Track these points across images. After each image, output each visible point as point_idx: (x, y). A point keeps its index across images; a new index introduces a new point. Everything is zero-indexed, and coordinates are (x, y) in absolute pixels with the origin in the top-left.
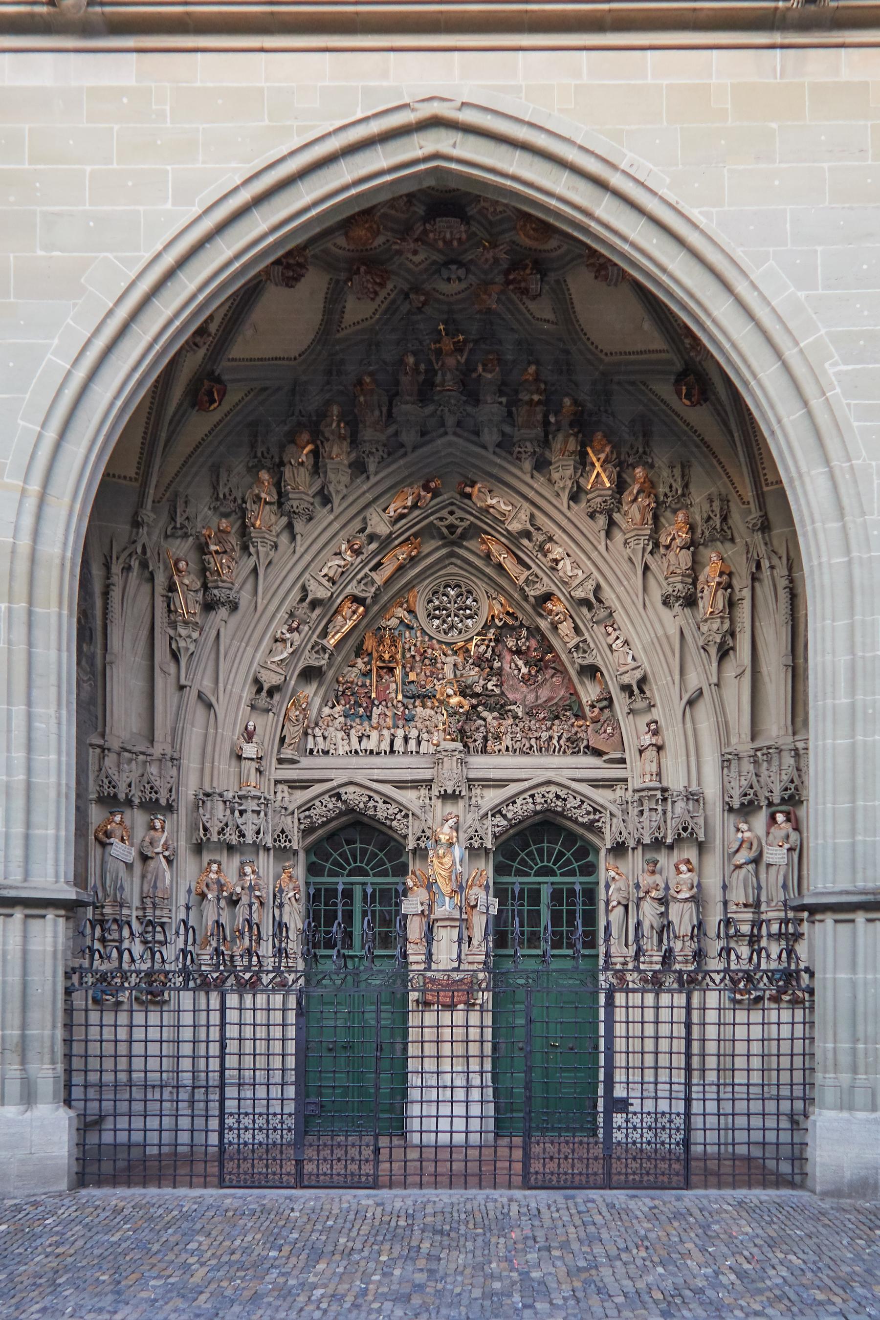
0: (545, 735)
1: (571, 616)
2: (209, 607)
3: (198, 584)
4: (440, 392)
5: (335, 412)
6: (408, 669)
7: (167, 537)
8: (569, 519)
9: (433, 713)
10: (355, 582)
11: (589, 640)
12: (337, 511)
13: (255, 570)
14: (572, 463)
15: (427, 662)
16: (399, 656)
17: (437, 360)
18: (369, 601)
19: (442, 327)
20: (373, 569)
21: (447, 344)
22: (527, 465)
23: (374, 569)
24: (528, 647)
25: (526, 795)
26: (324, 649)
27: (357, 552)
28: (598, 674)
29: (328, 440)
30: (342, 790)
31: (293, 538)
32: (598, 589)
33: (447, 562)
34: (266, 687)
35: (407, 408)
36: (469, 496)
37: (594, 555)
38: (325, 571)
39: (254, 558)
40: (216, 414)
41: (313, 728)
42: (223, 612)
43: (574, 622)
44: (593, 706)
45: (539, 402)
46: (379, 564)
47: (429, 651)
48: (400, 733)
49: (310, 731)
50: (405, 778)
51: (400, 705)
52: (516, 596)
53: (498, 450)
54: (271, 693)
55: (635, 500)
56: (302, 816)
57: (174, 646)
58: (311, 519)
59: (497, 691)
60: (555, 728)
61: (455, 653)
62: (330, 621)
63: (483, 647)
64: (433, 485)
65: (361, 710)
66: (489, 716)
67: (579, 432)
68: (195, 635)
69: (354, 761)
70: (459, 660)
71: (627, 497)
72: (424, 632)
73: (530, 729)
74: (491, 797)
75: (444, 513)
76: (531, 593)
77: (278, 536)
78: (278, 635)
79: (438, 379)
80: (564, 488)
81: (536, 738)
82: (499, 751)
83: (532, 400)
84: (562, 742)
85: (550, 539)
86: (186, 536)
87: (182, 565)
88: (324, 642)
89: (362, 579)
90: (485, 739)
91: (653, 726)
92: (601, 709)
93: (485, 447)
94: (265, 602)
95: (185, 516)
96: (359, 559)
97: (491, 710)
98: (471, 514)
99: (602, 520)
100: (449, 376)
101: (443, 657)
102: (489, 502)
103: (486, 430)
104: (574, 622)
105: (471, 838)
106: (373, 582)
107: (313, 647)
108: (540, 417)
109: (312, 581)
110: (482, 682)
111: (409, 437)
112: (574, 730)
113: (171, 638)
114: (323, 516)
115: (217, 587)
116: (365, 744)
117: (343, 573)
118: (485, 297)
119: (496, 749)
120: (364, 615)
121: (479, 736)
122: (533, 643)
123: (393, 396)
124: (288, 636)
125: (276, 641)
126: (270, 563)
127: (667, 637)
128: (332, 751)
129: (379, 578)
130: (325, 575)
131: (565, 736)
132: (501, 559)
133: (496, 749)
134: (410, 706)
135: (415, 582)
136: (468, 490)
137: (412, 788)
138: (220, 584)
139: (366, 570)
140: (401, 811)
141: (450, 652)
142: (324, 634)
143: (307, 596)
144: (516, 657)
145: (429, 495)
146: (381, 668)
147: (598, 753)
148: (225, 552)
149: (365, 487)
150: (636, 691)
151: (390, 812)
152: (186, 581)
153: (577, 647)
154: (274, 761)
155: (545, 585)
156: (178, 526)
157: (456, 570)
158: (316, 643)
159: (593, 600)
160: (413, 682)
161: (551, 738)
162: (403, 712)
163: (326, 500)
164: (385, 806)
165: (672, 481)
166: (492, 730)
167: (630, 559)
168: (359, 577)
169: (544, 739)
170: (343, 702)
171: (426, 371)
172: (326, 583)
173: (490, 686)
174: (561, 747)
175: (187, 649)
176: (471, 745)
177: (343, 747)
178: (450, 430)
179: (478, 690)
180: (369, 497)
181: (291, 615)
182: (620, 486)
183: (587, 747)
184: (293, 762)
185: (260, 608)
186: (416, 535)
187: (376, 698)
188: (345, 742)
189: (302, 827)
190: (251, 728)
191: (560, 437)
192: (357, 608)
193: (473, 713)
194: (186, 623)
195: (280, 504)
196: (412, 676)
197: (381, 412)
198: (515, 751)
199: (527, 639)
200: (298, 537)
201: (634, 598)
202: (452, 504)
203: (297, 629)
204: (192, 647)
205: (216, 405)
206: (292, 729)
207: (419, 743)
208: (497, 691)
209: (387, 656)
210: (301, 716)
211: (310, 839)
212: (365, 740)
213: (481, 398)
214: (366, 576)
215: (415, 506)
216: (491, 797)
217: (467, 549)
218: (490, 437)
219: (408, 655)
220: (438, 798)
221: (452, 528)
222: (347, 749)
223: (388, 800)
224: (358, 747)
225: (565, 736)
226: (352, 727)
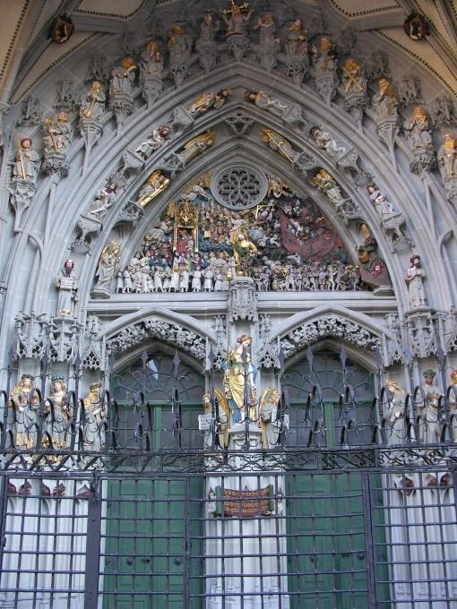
0: (322, 275)
1: (337, 184)
2: (44, 174)
3: (37, 157)
4: (230, 35)
5: (153, 48)
6: (203, 229)
7: (18, 125)
8: (333, 114)
9: (224, 262)
10: (162, 160)
11: (354, 200)
12: (151, 108)
13: (84, 149)
14: (332, 76)
15: (219, 223)
16: (196, 220)
17: (229, 19)
18: (173, 174)
20: (177, 152)
22: (298, 79)
23: (178, 152)
24: (301, 213)
25: (310, 322)
26: (135, 209)
27: (164, 136)
28: (364, 226)
29: (147, 62)
30: (146, 320)
31: (115, 126)
32: (359, 161)
33: (234, 153)
34: (85, 232)
35: (206, 42)
36: (253, 101)
37: (354, 138)
38: (138, 149)
39: (83, 139)
40: (66, 48)
41: (123, 273)
42: (55, 177)
43: (341, 189)
44: (361, 251)
46: (182, 149)
47: (221, 216)
48: (198, 274)
49: (120, 274)
50: (203, 309)
51: (197, 256)
52: (291, 174)
54: (88, 239)
55: (382, 100)
56: (110, 342)
57: (12, 201)
58: (130, 114)
59: (278, 245)
60: (330, 269)
61: (242, 217)
62: (141, 188)
63: (265, 213)
66: (273, 264)
67: (334, 59)
68: (31, 194)
69: (157, 296)
70: (246, 222)
71: (376, 98)
72: (216, 202)
73: (309, 271)
74: (279, 326)
75: (234, 115)
76: (305, 167)
77: (104, 125)
78: (99, 194)
80: (327, 93)
81: (315, 278)
82: (284, 288)
83: (299, 40)
84: (337, 281)
85: (317, 128)
86: (32, 124)
87: (26, 143)
88: (137, 203)
89: (169, 158)
90: (271, 280)
92: (369, 252)
93: (265, 69)
94: (90, 169)
95: (34, 111)
96: (167, 143)
97: (274, 259)
99: (358, 114)
101: (233, 221)
102: (269, 102)
104: (341, 189)
105: (263, 360)
106: (177, 160)
107: (126, 207)
109: (128, 155)
110: (265, 238)
111: (207, 62)
112: (346, 272)
113: (11, 195)
114: (140, 112)
115: (53, 158)
116: (167, 284)
117: (154, 151)
119: (281, 286)
120: (169, 185)
121: (266, 277)
122: (305, 211)
123: (198, 34)
124: (106, 194)
125: (97, 199)
126: (96, 144)
128: (138, 289)
129: (182, 158)
130: (139, 151)
131: (340, 275)
133: (281, 286)
134: (206, 257)
135: (210, 167)
136: (252, 96)
137: (208, 317)
138: (55, 155)
139: (172, 152)
140: (198, 337)
141: (238, 216)
142: (136, 197)
143: (123, 167)
144: (292, 220)
147: (369, 288)
148: (61, 134)
149: (173, 93)
151: (189, 337)
152: (28, 154)
153: (344, 206)
154: (88, 298)
155: (316, 162)
156: (27, 117)
157: (241, 160)
158: (129, 204)
159: (357, 168)
160: (208, 238)
161: (327, 277)
163: (141, 99)
164: (184, 333)
165: (407, 89)
167: (382, 142)
168: (166, 156)
169: (321, 277)
172: (140, 157)
173: (272, 241)
174: (336, 284)
175: (24, 204)
176: (260, 284)
177: (148, 286)
179: (263, 244)
180: (176, 100)
181: (110, 181)
182: (370, 92)
183: (358, 285)
184: (104, 296)
185: (85, 174)
186: (211, 129)
188: (150, 282)
189: (109, 352)
190: (69, 265)
191: (322, 59)
192: (164, 180)
193: (258, 261)
194: (24, 183)
195: (107, 103)
196: (207, 234)
197: (187, 47)
198: (297, 288)
199: (301, 207)
200: (120, 125)
201: (390, 165)
202: (240, 108)
203: (114, 190)
204: (27, 203)
205: (65, 39)
206: (105, 270)
207: (214, 283)
208: (278, 245)
209: (186, 220)
210: (113, 261)
211: (117, 364)
212: (167, 281)
214: (172, 156)
215: (211, 108)
216: (279, 326)
217: (251, 142)
218: (268, 62)
219: (204, 219)
220: (232, 324)
221: (239, 126)
222: (152, 287)
223: (187, 327)
224: (161, 286)
225: (338, 278)
226: (156, 270)
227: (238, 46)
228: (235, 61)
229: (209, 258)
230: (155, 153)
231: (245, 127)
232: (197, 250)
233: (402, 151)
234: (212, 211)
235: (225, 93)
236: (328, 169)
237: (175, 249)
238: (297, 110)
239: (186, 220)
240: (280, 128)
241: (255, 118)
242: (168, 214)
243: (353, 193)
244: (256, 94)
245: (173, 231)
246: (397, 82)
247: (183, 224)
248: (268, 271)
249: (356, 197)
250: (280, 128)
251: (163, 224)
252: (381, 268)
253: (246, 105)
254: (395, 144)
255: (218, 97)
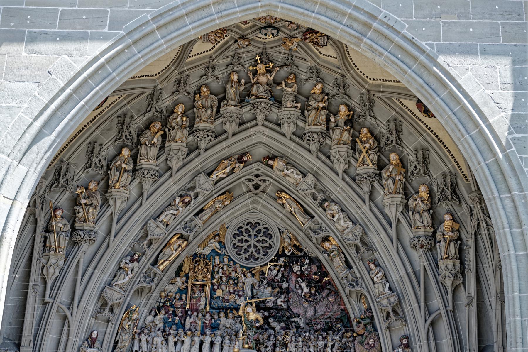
19: (258, 58)
20: (197, 214)
21: (261, 68)
45: (324, 108)
46: (202, 210)
51: (208, 315)
53: (293, 137)
55: (389, 176)
60: (329, 338)
64: (245, 158)
65: (177, 318)
71: (385, 174)
79: (254, 91)
81: (314, 346)
91: (405, 341)
93: (285, 136)
98: (272, 178)
100: (261, 89)
103: (286, 125)
108: (324, 117)
118: (289, 44)
127: (415, 272)
132: (292, 210)
134: (216, 317)
136: (270, 162)
145: (242, 165)
146: (194, 285)
150: (391, 315)
161: (326, 346)
162: (210, 321)
166: (280, 338)
170: (163, 312)
171: (245, 84)
178: (260, 123)
187: (191, 309)
213: (283, 103)
215: (232, 172)
227: (260, 111)
228: (257, 125)
229: (219, 317)
230: (176, 219)
231: (262, 188)
232: (208, 309)
233: (403, 225)
234: (225, 268)
235: (245, 158)
236: (335, 238)
237: (188, 307)
238: (310, 178)
239: (200, 277)
240: (294, 193)
241: (272, 180)
242: (183, 270)
243: (356, 265)
244: (274, 158)
245: (187, 287)
246: (408, 153)
247: (197, 280)
248: (272, 338)
249: (357, 268)
250: (294, 193)
251: (178, 279)
252: (374, 341)
253: (263, 169)
254: (398, 219)
255: (238, 165)
